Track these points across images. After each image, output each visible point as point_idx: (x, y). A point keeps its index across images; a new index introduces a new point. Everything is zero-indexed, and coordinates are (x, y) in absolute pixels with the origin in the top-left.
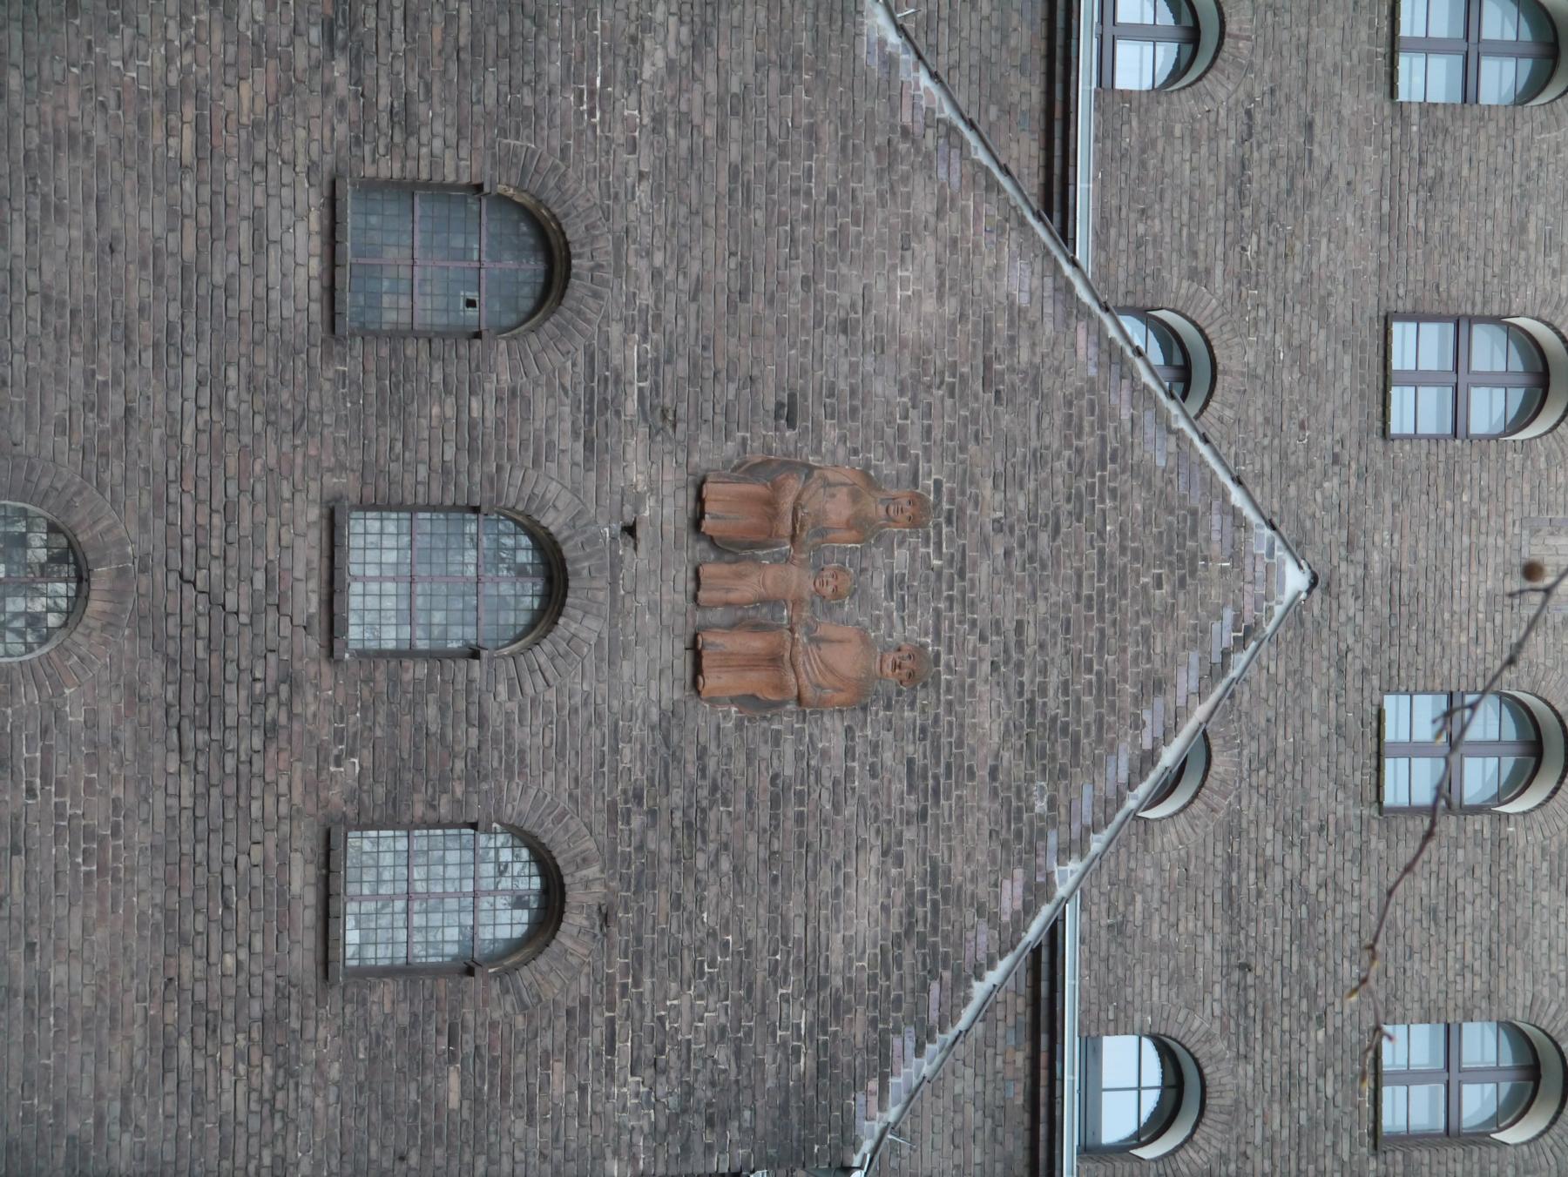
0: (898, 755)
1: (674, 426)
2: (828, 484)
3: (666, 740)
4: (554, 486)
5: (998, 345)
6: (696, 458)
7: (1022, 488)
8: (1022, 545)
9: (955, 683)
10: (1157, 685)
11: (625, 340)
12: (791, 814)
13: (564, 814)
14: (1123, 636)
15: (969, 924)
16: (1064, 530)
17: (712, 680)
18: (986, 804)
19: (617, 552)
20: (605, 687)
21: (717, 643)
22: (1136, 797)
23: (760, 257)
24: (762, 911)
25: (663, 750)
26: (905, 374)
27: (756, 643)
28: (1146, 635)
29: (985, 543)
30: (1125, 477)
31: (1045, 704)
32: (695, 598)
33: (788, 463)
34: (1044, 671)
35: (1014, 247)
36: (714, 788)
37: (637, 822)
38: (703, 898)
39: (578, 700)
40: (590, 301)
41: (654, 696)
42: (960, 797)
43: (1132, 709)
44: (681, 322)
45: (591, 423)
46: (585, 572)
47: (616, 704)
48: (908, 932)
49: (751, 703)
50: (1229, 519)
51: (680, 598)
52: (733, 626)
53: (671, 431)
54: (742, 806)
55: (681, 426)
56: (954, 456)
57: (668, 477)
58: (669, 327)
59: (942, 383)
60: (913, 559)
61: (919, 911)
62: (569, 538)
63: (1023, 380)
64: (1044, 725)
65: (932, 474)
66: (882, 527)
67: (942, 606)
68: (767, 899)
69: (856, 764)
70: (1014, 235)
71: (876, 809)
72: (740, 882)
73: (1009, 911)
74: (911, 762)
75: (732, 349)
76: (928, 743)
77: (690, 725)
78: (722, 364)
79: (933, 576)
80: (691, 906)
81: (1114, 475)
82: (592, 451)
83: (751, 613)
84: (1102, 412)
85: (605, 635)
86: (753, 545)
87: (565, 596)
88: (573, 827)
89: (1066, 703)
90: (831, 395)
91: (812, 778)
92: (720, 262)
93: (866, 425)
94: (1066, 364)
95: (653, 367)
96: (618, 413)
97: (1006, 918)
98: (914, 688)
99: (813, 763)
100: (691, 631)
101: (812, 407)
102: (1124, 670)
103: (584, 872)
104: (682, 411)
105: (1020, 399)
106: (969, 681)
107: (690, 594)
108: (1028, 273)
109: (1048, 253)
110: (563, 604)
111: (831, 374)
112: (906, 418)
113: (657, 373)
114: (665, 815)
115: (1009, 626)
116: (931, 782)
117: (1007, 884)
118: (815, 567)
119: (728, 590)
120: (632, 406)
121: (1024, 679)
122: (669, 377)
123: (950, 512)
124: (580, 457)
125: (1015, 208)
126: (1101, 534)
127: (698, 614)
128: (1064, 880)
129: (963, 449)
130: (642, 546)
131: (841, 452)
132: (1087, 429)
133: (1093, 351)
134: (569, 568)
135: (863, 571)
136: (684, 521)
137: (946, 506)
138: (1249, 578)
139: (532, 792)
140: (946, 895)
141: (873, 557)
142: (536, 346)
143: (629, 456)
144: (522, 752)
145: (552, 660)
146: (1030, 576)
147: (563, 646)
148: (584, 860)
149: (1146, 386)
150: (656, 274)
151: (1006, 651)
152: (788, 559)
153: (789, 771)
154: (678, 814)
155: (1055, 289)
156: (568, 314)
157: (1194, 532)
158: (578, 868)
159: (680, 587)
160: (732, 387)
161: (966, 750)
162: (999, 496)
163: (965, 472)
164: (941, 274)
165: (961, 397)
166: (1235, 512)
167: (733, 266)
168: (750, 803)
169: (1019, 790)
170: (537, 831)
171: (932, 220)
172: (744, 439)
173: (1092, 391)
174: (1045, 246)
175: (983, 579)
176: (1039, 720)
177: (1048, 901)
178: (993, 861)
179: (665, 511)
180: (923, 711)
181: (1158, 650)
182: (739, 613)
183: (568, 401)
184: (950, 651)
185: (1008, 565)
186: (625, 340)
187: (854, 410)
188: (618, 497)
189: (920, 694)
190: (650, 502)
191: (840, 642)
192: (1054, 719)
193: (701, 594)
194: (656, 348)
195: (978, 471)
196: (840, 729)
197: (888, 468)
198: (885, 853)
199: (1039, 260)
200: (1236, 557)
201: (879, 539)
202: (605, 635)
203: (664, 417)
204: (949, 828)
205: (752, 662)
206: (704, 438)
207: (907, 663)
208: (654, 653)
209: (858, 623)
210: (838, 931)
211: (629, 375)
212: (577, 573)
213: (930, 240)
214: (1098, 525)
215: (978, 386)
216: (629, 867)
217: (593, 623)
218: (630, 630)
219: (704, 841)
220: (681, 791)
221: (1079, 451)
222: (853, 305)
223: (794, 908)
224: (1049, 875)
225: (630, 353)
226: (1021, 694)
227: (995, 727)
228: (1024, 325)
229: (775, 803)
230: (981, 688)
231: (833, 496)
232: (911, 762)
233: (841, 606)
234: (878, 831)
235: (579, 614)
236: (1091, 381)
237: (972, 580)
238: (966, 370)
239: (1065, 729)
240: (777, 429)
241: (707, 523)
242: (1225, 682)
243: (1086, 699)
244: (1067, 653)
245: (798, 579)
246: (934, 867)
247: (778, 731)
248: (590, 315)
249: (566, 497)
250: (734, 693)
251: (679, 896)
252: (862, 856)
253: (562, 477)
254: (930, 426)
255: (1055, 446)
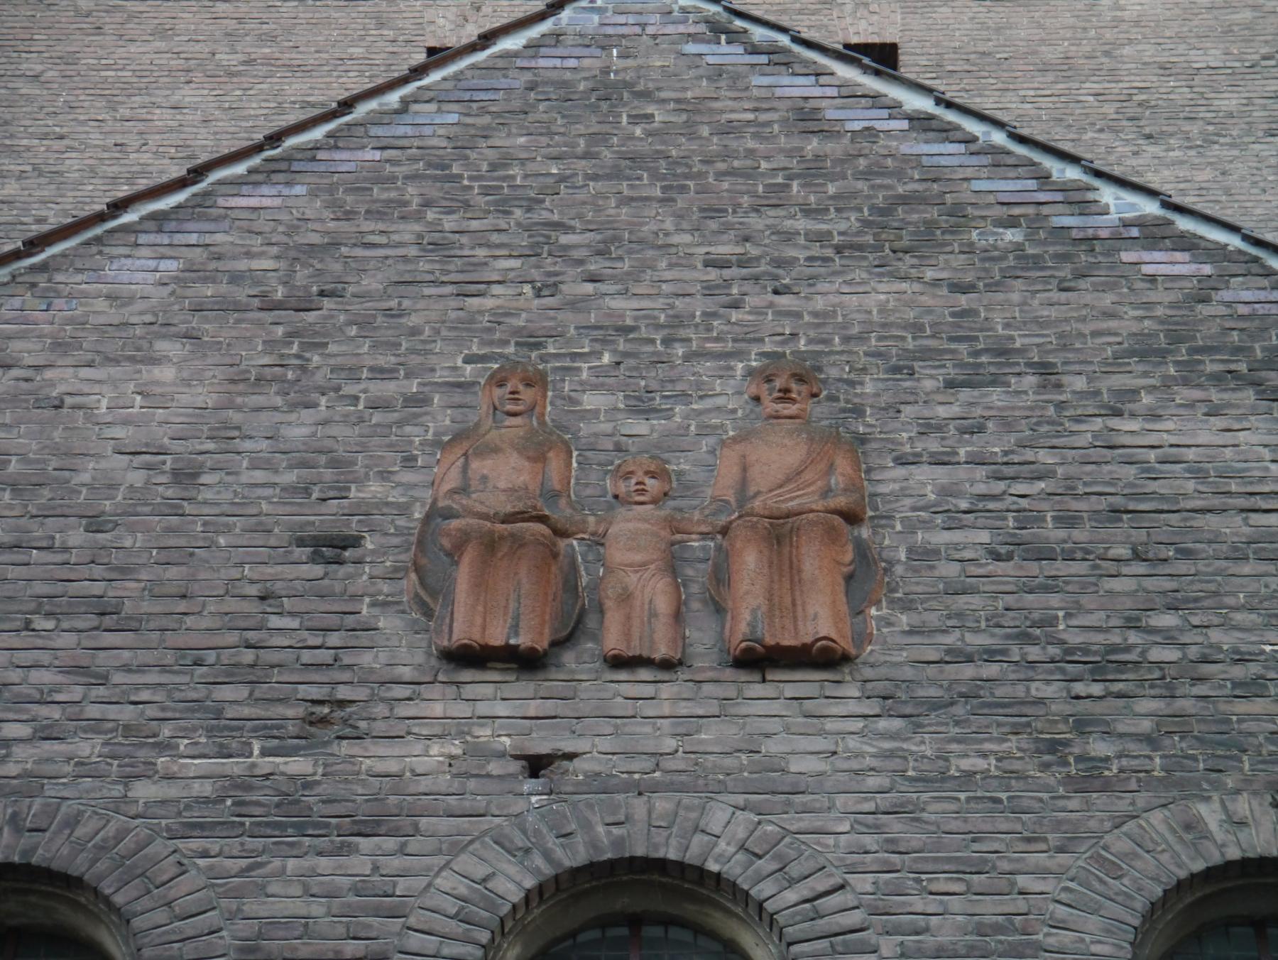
0: (940, 398)
1: (342, 704)
2: (463, 490)
3: (935, 705)
4: (446, 881)
5: (241, 293)
6: (406, 673)
7: (486, 264)
8: (580, 262)
9: (812, 334)
10: (806, 118)
11: (169, 777)
12: (1062, 534)
13: (1098, 859)
14: (726, 155)
15: (1223, 310)
16: (556, 217)
17: (819, 620)
18: (1016, 297)
19: (578, 783)
20: (840, 800)
21: (750, 616)
22: (988, 133)
23: (40, 588)
24: (1247, 569)
25: (959, 710)
26: (279, 401)
27: (750, 561)
28: (729, 129)
29: (575, 304)
30: (473, 155)
31: (840, 234)
32: (667, 665)
33: (421, 543)
34: (789, 237)
35: (79, 278)
36: (1025, 638)
37: (1100, 747)
38: (1236, 651)
39: (869, 841)
40: (80, 832)
41: (859, 724)
42: (1007, 326)
43: (846, 140)
44: (145, 695)
45: (327, 825)
46: (616, 831)
47: (873, 782)
48: (1256, 384)
49: (862, 578)
50: (543, 51)
51: (666, 691)
52: (719, 609)
53: (353, 709)
54: (1055, 600)
55: (343, 693)
56: (424, 342)
57: (438, 709)
58: (151, 711)
59: (298, 356)
60: (595, 387)
61: (1210, 368)
62: (547, 855)
63: (305, 265)
64: (874, 235)
65: (451, 363)
66: (542, 423)
67: (680, 352)
68: (1224, 563)
69: (962, 452)
70: (59, 277)
71: (1038, 424)
72: (1196, 600)
73: (1194, 267)
74: (951, 384)
75: (205, 623)
76: (916, 365)
77: (908, 673)
78: (233, 638)
79: (632, 362)
80: (1254, 669)
81: (467, 166)
82: (378, 823)
83: (695, 588)
84: (365, 180)
85: (740, 799)
86: (570, 584)
87: (662, 865)
88: (1124, 845)
89: (838, 210)
90: (307, 492)
91: (991, 506)
92: (39, 642)
93: (363, 449)
94: (284, 217)
95: (224, 733)
96: (307, 786)
97: (1207, 269)
98: (824, 382)
99: (964, 505)
100: (729, 673)
101: (325, 518)
102: (781, 150)
103: (1213, 826)
104: (315, 692)
105: (337, 267)
106: (807, 318)
107: (661, 676)
108: (129, 262)
109: (98, 240)
110: (681, 867)
111: (268, 492)
112: (357, 398)
113: (240, 728)
114: (1082, 706)
115: (713, 274)
116: (984, 359)
117: (1148, 269)
118: (611, 508)
119: (653, 614)
120: (298, 765)
121: (802, 255)
122: (246, 711)
123: (517, 344)
124: (390, 843)
125: (14, 277)
126: (562, 179)
127: (698, 664)
128: (1133, 206)
129: (414, 332)
130: (568, 746)
131: (408, 477)
132: (393, 194)
133: (265, 190)
134: (609, 855)
135: (619, 448)
136: (525, 687)
137: (511, 349)
138: (638, 30)
139: (1061, 911)
140: (1176, 338)
141: (596, 435)
142: (160, 916)
143: (393, 767)
144: (980, 931)
145: (792, 882)
146: (630, 252)
147: (766, 865)
148: (1188, 827)
149: (329, 135)
150: (46, 734)
151: (756, 278)
152: (598, 541)
153: (984, 536)
154: (1079, 688)
155: (160, 231)
156: (101, 866)
157: (564, 84)
158: (1207, 836)
159: (648, 690)
160: (275, 622)
161: (926, 320)
162: (497, 289)
163: (451, 329)
164: (116, 361)
165: (324, 336)
166: (532, 46)
167: (50, 624)
168: (1046, 589)
169: (983, 260)
170: (1140, 904)
171: (15, 372)
172: (373, 605)
173: (332, 189)
174: (87, 243)
175: (635, 304)
176: (869, 239)
177: (1170, 223)
178: (1112, 287)
179: (502, 711)
180: (864, 370)
181: (750, 116)
182: (695, 605)
183: (277, 863)
184: (761, 340)
185: (615, 279)
186: (169, 777)
187: (335, 463)
188: (472, 784)
189: (834, 373)
190: (484, 733)
191: (744, 469)
192: (866, 223)
193: (657, 656)
194: (187, 733)
195: (453, 315)
196: (901, 472)
197: (441, 419)
198: (1118, 413)
199: (106, 250)
200: (603, 43)
201: (565, 429)
202: (740, 799)
203: (324, 721)
204: (1061, 336)
205: (784, 568)
206: (366, 659)
207: (778, 383)
208: (773, 725)
209: (712, 452)
210: (1267, 469)
211: (237, 771)
212: (618, 843)
213: (49, 374)
214: (551, 180)
215: (311, 317)
216: (1194, 758)
217: (717, 817)
218: (729, 762)
219: (1128, 649)
220: (1034, 685)
221: (427, 204)
222: (149, 467)
223: (1232, 527)
224: (1126, 224)
225: (195, 770)
226: (826, 259)
227: (883, 287)
228: (213, 265)
229: (1043, 555)
230: (819, 303)
231: (484, 479)
232: (951, 384)
233: (680, 474)
234: (1077, 419)
235: (698, 840)
236: (313, 194)
237: (636, 319)
238: (280, 331)
239: (883, 212)
240: (359, 562)
241: (523, 640)
242: (797, 49)
243: (831, 189)
244: (757, 211)
245: (631, 537)
246: (1132, 353)
247: (910, 550)
248: (111, 829)
249: (465, 862)
250: (844, 608)
251: (1236, 685)
252: (1127, 440)
253: (429, 869)
254: (372, 369)
255: (417, 228)
